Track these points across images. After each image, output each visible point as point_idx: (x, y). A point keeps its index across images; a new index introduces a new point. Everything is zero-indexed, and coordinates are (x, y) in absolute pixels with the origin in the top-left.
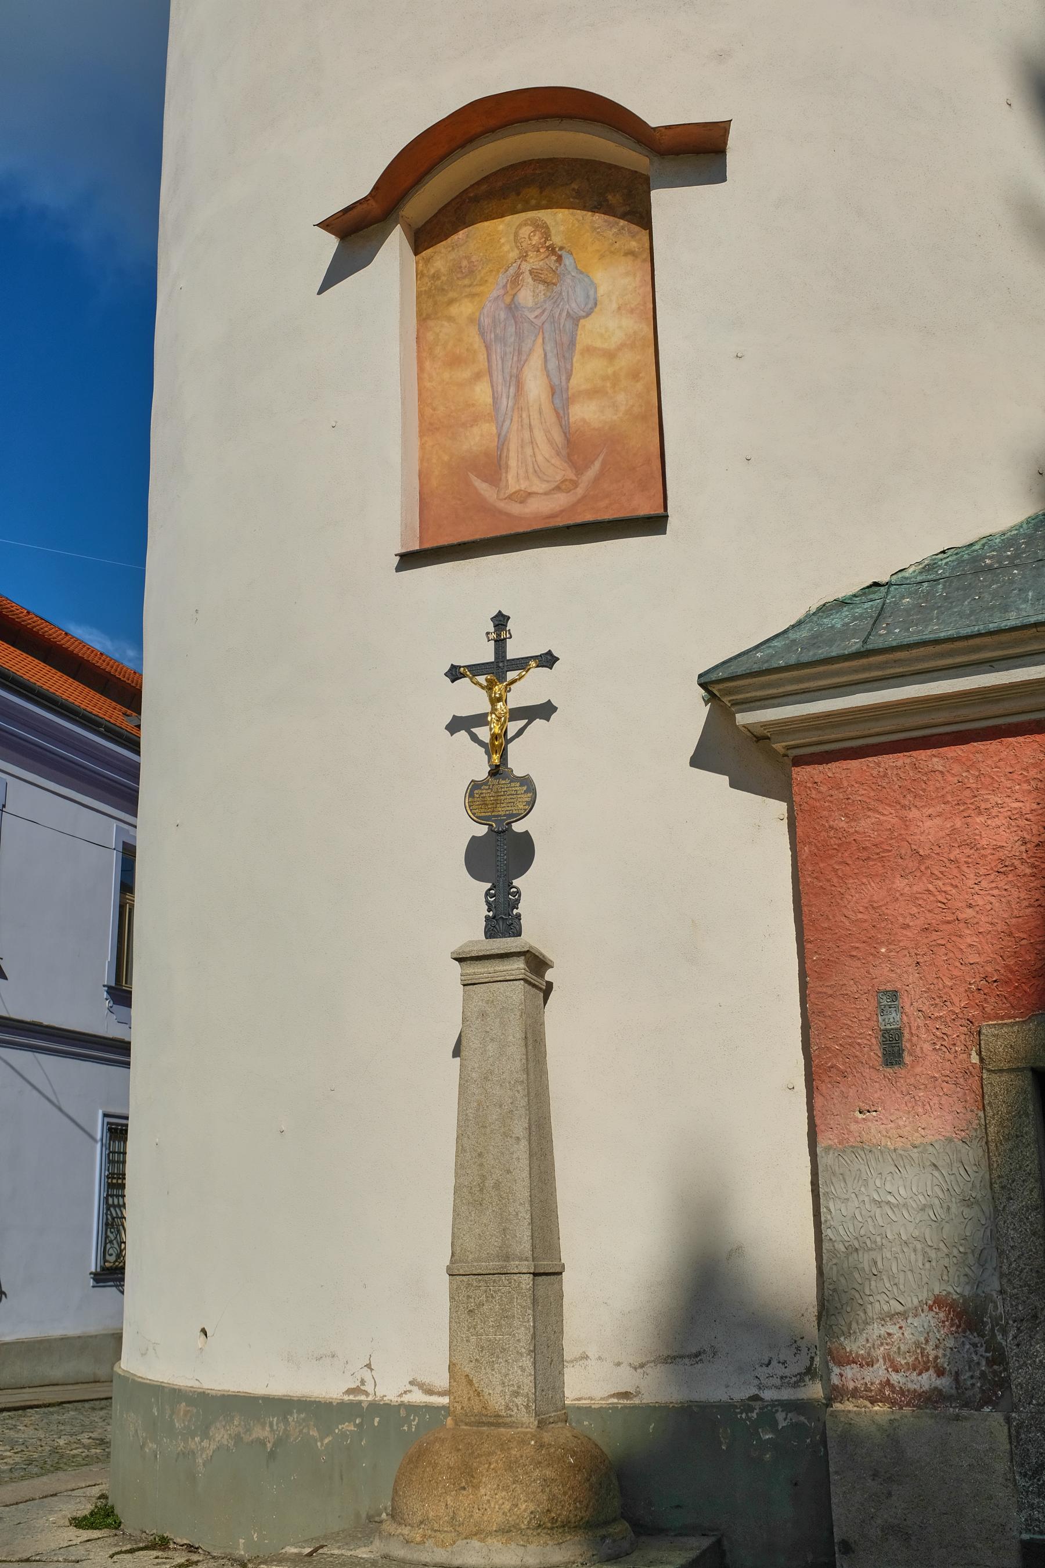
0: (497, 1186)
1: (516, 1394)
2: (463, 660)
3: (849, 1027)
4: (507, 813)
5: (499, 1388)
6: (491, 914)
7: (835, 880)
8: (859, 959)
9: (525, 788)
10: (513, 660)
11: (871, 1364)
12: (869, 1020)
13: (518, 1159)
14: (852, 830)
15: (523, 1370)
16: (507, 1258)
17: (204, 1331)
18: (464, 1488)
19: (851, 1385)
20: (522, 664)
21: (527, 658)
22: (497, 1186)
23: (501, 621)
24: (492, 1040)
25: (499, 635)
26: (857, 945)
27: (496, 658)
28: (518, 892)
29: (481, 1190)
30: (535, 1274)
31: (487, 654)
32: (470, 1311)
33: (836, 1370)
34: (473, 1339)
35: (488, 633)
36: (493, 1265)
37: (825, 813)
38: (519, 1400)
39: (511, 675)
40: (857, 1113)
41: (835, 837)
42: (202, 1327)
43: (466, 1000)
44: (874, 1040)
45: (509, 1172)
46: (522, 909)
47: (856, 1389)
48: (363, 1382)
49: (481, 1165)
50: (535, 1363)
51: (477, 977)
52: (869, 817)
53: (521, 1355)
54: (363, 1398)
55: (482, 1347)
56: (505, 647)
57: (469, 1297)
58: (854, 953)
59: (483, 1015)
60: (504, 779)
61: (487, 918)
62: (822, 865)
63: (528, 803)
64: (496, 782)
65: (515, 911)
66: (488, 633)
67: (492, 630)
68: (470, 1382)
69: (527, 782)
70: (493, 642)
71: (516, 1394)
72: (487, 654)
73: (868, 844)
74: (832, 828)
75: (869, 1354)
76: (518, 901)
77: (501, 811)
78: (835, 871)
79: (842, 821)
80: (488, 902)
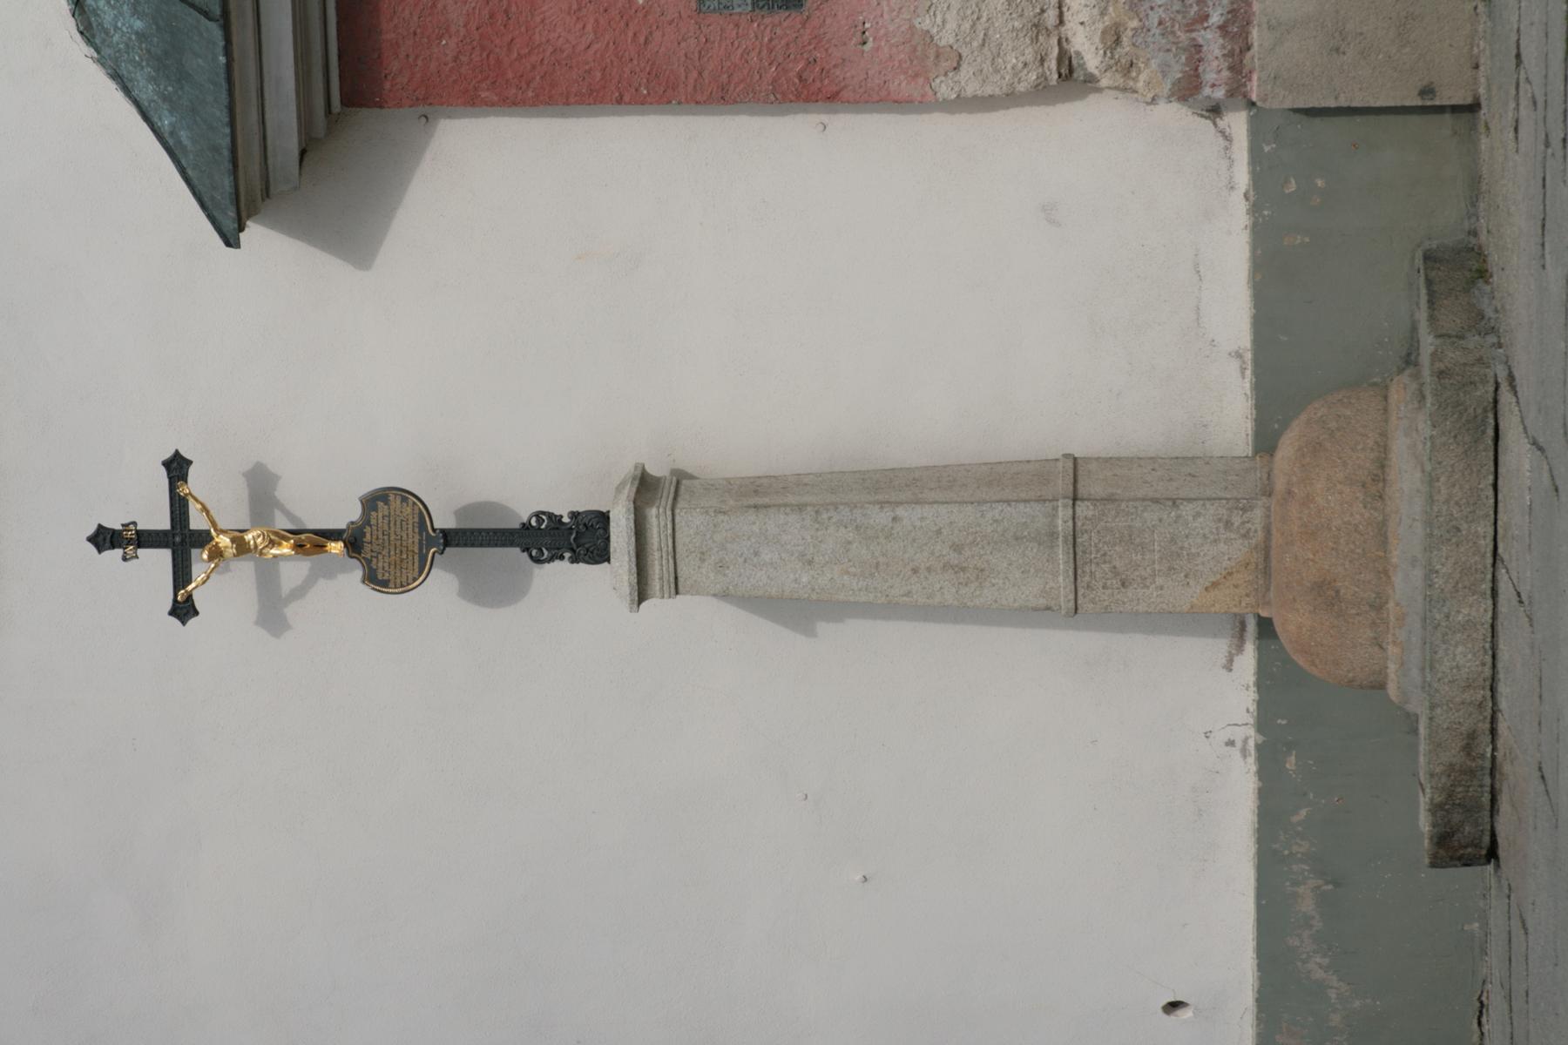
0: (957, 548)
1: (1228, 524)
2: (165, 596)
3: (747, 52)
4: (417, 530)
5: (1222, 547)
6: (567, 555)
7: (534, 59)
8: (651, 33)
9: (380, 504)
10: (172, 520)
11: (1198, 47)
12: (737, 25)
13: (922, 519)
14: (463, 32)
15: (1198, 514)
16: (1053, 535)
17: (1173, 1006)
18: (1338, 592)
19: (1226, 74)
20: (179, 507)
21: (171, 499)
22: (957, 548)
23: (104, 539)
24: (756, 554)
25: (130, 541)
26: (630, 34)
27: (166, 546)
28: (538, 515)
29: (963, 569)
30: (1075, 499)
31: (159, 561)
32: (1123, 584)
33: (1207, 91)
34: (1159, 581)
35: (125, 559)
36: (1062, 554)
37: (433, 66)
38: (1237, 521)
39: (197, 522)
40: (867, 47)
41: (471, 54)
42: (1160, 1011)
43: (696, 590)
44: (767, 20)
45: (939, 532)
46: (563, 510)
47: (1231, 68)
48: (1231, 743)
49: (929, 569)
50: (1190, 500)
51: (666, 575)
52: (445, 7)
53: (1179, 517)
54: (1251, 743)
55: (1170, 569)
56: (150, 533)
57: (1104, 587)
58: (642, 40)
59: (721, 566)
60: (364, 535)
61: (574, 560)
62: (510, 75)
63: (404, 500)
64: (367, 548)
65: (566, 520)
66: (125, 559)
67: (118, 552)
68: (1215, 585)
69: (374, 501)
70: (141, 552)
71: (1228, 524)
72: (159, 561)
73: (486, 12)
74: (456, 59)
75: (1185, 50)
76: (550, 516)
77: (413, 540)
78: (520, 57)
79: (447, 44)
80: (551, 560)
